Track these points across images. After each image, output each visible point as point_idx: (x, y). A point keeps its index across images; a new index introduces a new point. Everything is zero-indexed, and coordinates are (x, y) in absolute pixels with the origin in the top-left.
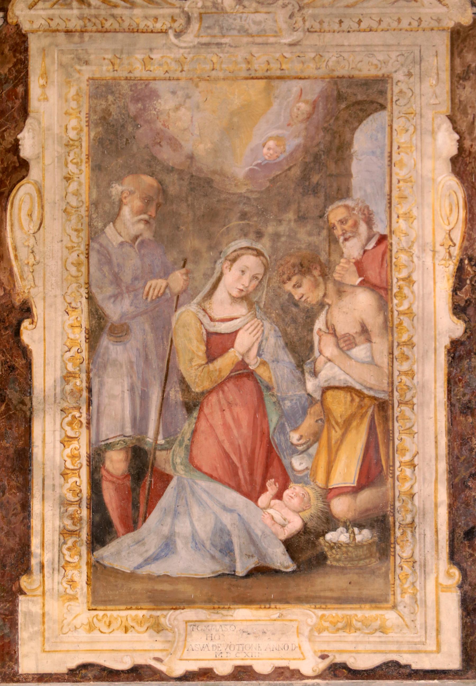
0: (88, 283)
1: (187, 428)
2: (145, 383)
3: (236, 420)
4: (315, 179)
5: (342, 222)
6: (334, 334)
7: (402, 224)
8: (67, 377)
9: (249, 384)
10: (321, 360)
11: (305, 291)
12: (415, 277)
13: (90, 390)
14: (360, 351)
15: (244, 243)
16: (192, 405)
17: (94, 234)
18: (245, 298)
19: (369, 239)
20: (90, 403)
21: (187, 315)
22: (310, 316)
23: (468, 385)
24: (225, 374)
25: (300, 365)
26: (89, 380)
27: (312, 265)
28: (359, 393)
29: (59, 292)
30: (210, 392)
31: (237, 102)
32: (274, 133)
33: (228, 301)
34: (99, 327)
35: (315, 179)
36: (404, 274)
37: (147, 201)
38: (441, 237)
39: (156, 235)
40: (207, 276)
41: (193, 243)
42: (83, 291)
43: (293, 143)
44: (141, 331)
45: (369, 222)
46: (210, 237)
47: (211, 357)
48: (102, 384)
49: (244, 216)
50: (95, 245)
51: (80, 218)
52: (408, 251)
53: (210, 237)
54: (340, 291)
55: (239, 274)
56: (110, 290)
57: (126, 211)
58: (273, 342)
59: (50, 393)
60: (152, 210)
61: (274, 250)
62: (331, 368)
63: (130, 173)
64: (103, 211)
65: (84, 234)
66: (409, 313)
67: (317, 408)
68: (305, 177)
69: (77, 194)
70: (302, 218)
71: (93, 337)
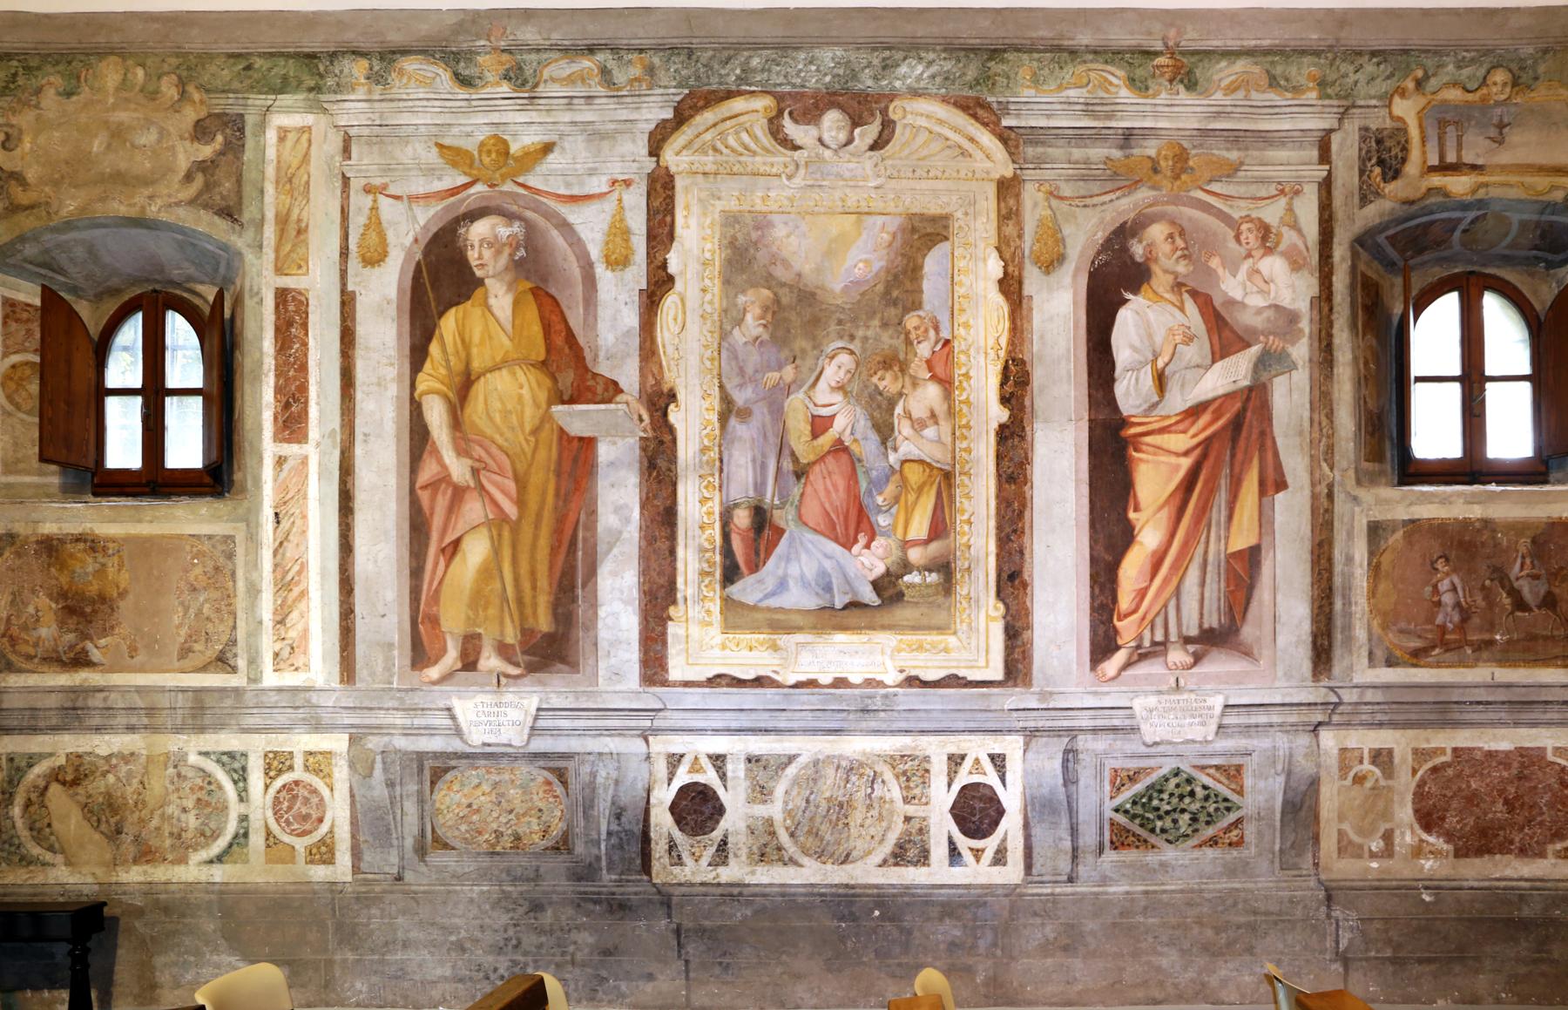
0: (720, 375)
1: (796, 491)
2: (764, 455)
3: (835, 486)
4: (895, 293)
5: (916, 328)
6: (910, 418)
7: (961, 331)
8: (704, 450)
9: (844, 457)
10: (900, 438)
11: (887, 383)
12: (972, 373)
13: (721, 461)
14: (930, 432)
15: (840, 344)
16: (801, 473)
17: (724, 335)
18: (841, 388)
19: (936, 343)
20: (721, 471)
21: (796, 401)
22: (892, 404)
23: (1011, 459)
24: (826, 449)
25: (884, 442)
26: (721, 453)
27: (893, 362)
28: (929, 465)
29: (697, 382)
30: (814, 463)
31: (834, 232)
32: (864, 256)
33: (828, 390)
34: (728, 410)
35: (895, 293)
36: (963, 371)
37: (766, 309)
38: (991, 342)
39: (772, 336)
40: (812, 370)
41: (801, 343)
42: (716, 381)
43: (879, 264)
44: (761, 414)
45: (937, 329)
46: (814, 338)
47: (815, 435)
48: (730, 456)
49: (840, 322)
50: (724, 344)
51: (713, 322)
52: (966, 352)
53: (814, 338)
54: (915, 384)
55: (836, 369)
56: (737, 380)
57: (749, 317)
58: (863, 424)
59: (690, 462)
60: (769, 317)
61: (864, 350)
62: (908, 445)
63: (753, 286)
64: (730, 318)
65: (716, 335)
66: (967, 402)
67: (897, 477)
68: (887, 292)
69: (711, 302)
70: (885, 325)
71: (724, 418)
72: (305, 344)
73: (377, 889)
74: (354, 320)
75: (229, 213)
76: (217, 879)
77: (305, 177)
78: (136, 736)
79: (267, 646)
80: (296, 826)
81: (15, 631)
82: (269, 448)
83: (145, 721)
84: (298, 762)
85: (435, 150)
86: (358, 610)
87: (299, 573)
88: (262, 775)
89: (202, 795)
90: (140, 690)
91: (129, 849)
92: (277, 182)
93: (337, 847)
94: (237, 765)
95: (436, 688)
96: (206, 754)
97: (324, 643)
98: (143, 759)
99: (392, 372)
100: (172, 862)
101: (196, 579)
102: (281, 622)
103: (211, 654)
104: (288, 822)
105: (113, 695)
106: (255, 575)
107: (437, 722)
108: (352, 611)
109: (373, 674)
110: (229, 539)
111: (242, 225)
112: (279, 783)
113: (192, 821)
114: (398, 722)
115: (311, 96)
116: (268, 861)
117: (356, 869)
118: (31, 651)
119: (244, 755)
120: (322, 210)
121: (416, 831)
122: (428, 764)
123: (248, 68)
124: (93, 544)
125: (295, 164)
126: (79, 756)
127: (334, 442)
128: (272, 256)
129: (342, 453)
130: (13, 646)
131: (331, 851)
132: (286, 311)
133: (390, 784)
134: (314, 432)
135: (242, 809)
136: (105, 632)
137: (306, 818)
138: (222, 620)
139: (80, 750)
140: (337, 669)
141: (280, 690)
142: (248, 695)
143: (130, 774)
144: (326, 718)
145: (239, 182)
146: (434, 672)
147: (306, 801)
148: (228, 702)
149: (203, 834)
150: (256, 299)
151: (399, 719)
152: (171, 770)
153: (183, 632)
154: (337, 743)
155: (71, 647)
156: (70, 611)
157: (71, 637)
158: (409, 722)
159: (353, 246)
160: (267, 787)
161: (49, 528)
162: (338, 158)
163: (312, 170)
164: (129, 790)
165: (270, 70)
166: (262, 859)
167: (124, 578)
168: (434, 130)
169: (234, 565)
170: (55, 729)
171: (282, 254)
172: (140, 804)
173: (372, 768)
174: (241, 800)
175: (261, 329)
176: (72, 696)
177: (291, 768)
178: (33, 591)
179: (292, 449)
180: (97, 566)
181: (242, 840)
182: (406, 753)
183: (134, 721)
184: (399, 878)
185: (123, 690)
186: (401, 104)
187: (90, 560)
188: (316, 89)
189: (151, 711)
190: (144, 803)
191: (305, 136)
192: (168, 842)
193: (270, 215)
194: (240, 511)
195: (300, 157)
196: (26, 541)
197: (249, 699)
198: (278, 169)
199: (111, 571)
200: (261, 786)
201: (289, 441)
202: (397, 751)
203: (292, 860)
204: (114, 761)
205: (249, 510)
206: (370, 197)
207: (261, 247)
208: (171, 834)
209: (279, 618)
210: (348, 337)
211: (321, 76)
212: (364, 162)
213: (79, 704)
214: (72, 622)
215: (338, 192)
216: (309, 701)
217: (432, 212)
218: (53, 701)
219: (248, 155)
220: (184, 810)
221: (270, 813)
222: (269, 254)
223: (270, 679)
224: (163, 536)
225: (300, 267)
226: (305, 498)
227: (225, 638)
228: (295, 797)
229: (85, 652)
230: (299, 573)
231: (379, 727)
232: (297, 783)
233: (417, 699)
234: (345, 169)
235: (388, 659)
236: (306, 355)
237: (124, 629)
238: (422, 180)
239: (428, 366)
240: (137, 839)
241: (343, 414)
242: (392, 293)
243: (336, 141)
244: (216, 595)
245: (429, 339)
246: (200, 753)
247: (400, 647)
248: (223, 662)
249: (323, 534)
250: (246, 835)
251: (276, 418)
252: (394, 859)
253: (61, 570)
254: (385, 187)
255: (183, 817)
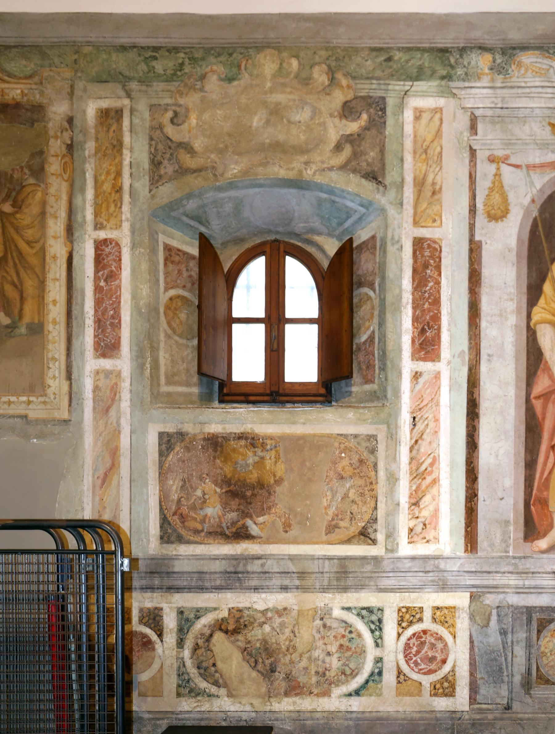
72: (438, 283)
73: (490, 716)
74: (480, 264)
75: (375, 176)
76: (355, 709)
77: (439, 149)
78: (289, 595)
79: (403, 522)
80: (423, 666)
81: (185, 510)
82: (408, 365)
83: (297, 582)
84: (427, 615)
85: (548, 129)
86: (481, 494)
87: (432, 464)
88: (395, 625)
89: (344, 642)
90: (292, 558)
91: (281, 684)
92: (415, 152)
93: (458, 683)
94: (374, 618)
95: (545, 556)
96: (349, 609)
97: (451, 521)
98: (294, 613)
99: (511, 306)
100: (318, 695)
101: (343, 469)
102: (416, 504)
103: (354, 529)
104: (416, 664)
105: (269, 562)
106: (394, 467)
107: (544, 583)
108: (476, 495)
109: (492, 545)
110: (371, 438)
111: (385, 187)
112: (410, 632)
113: (335, 663)
114: (512, 582)
115: (443, 83)
116: (399, 693)
117: (473, 700)
118: (199, 527)
119: (381, 610)
120: (453, 174)
121: (523, 669)
122: (536, 616)
123: (389, 59)
124: (253, 441)
125: (429, 138)
126: (240, 610)
127: (463, 361)
128: (411, 212)
129: (470, 369)
130: (183, 522)
131: (453, 686)
132: (423, 256)
133: (503, 633)
134: (445, 352)
135: (378, 653)
136: (262, 512)
137: (432, 659)
138: (365, 503)
139: (241, 606)
140: (463, 541)
141: (413, 558)
142: (385, 563)
143: (283, 625)
144: (451, 579)
145: (382, 151)
146: (543, 544)
147: (433, 646)
148: (369, 568)
149: (343, 673)
150: (397, 246)
151: (513, 581)
152: (318, 622)
153: (331, 512)
154: (461, 600)
155: (233, 523)
156: (233, 494)
157: (233, 515)
158: (521, 583)
159: (480, 205)
160: (399, 635)
161: (215, 428)
162: (466, 134)
163: (444, 142)
164: (282, 638)
165: (407, 61)
166: (394, 692)
167: (280, 469)
168: (548, 112)
169: (376, 458)
170: (219, 588)
171: (419, 211)
172: (291, 648)
173: (489, 620)
174: (377, 645)
175: (401, 270)
176: (234, 562)
177: (421, 620)
178: (201, 478)
179: (426, 367)
180: (257, 459)
181: (376, 677)
182: (517, 608)
183: (287, 582)
184: (508, 708)
185: (279, 558)
186: (520, 91)
187: (250, 454)
188: (448, 77)
189: (302, 575)
190: (294, 647)
191: (438, 116)
192: (314, 679)
193: (409, 179)
194: (382, 416)
195: (433, 132)
196: (194, 438)
197: (386, 565)
198: (415, 141)
199: (268, 463)
200: (394, 634)
201: (424, 360)
202: (509, 606)
203: (419, 693)
204: (269, 614)
205: (390, 415)
206: (494, 166)
207: (401, 204)
208: (317, 673)
209: (414, 501)
210: (475, 278)
211: (452, 67)
212: (489, 138)
213: (240, 569)
214: (234, 503)
215: (467, 161)
216: (437, 567)
217: (547, 178)
218: (218, 566)
219: (389, 130)
220: (329, 654)
221: (401, 656)
222: (409, 209)
223: (405, 549)
224: (314, 435)
225: (434, 221)
226: (438, 405)
227: (367, 517)
228: (423, 644)
229: (245, 527)
230: (432, 464)
231: (496, 587)
232: (425, 632)
233: (529, 565)
234: (472, 143)
235: (505, 533)
236: (439, 292)
237: (280, 508)
238: (538, 153)
239: (542, 301)
240: (288, 677)
241: (470, 339)
242: (513, 242)
243: (464, 121)
244: (361, 482)
245: (543, 280)
246: (343, 608)
247: (516, 523)
248: (365, 535)
249: (453, 433)
250: (380, 673)
251: (413, 341)
252: (504, 692)
253: (225, 461)
254: (507, 157)
255: (328, 659)
